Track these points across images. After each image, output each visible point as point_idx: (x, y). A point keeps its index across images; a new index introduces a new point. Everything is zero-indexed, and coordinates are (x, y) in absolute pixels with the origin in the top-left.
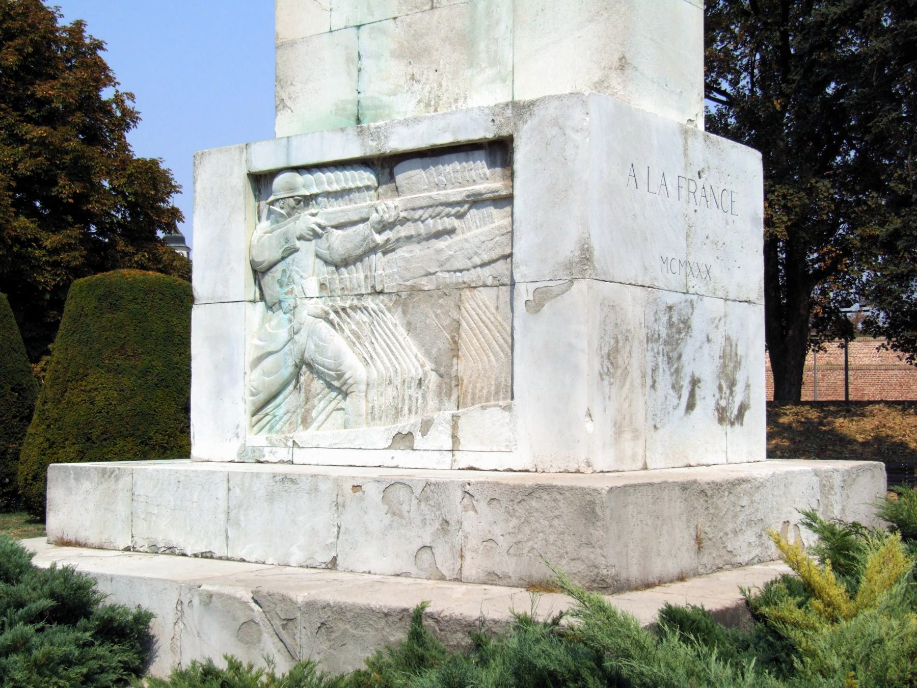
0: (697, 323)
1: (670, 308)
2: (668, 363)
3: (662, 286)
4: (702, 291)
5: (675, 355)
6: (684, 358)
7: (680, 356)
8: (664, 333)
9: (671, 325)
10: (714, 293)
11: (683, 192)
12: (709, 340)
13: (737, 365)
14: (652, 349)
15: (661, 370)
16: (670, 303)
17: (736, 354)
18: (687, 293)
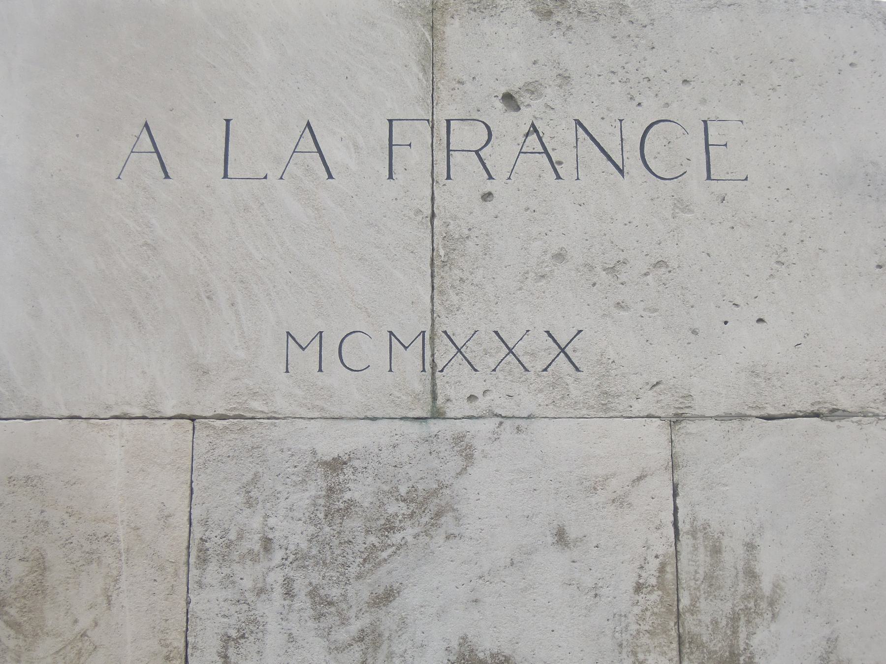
0: (495, 493)
1: (336, 465)
2: (319, 617)
3: (281, 405)
4: (528, 403)
5: (361, 591)
6: (410, 598)
7: (386, 597)
8: (294, 534)
9: (334, 508)
10: (605, 408)
11: (414, 159)
12: (561, 537)
13: (759, 602)
14: (229, 581)
15: (274, 639)
16: (329, 449)
17: (751, 575)
18: (437, 414)
